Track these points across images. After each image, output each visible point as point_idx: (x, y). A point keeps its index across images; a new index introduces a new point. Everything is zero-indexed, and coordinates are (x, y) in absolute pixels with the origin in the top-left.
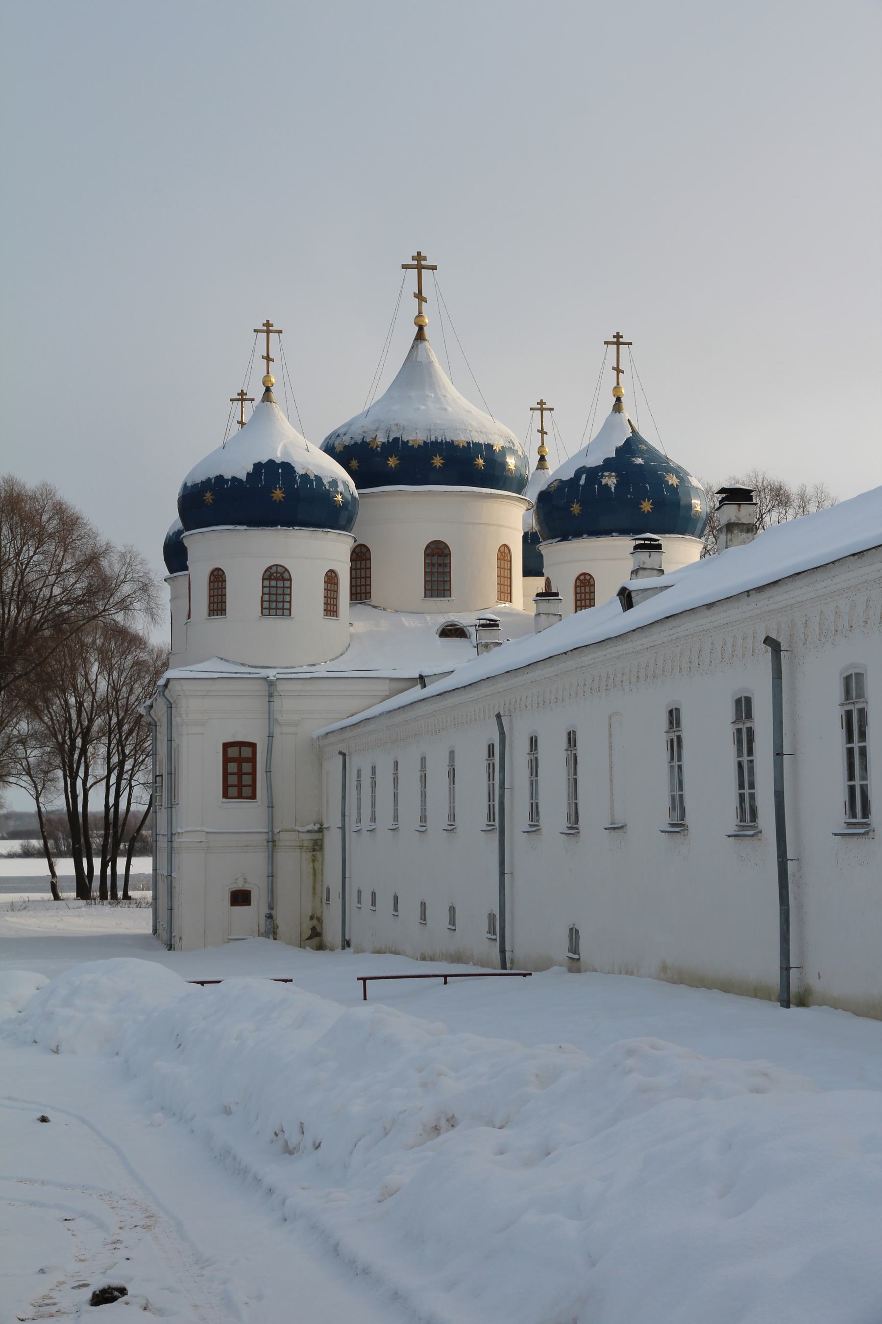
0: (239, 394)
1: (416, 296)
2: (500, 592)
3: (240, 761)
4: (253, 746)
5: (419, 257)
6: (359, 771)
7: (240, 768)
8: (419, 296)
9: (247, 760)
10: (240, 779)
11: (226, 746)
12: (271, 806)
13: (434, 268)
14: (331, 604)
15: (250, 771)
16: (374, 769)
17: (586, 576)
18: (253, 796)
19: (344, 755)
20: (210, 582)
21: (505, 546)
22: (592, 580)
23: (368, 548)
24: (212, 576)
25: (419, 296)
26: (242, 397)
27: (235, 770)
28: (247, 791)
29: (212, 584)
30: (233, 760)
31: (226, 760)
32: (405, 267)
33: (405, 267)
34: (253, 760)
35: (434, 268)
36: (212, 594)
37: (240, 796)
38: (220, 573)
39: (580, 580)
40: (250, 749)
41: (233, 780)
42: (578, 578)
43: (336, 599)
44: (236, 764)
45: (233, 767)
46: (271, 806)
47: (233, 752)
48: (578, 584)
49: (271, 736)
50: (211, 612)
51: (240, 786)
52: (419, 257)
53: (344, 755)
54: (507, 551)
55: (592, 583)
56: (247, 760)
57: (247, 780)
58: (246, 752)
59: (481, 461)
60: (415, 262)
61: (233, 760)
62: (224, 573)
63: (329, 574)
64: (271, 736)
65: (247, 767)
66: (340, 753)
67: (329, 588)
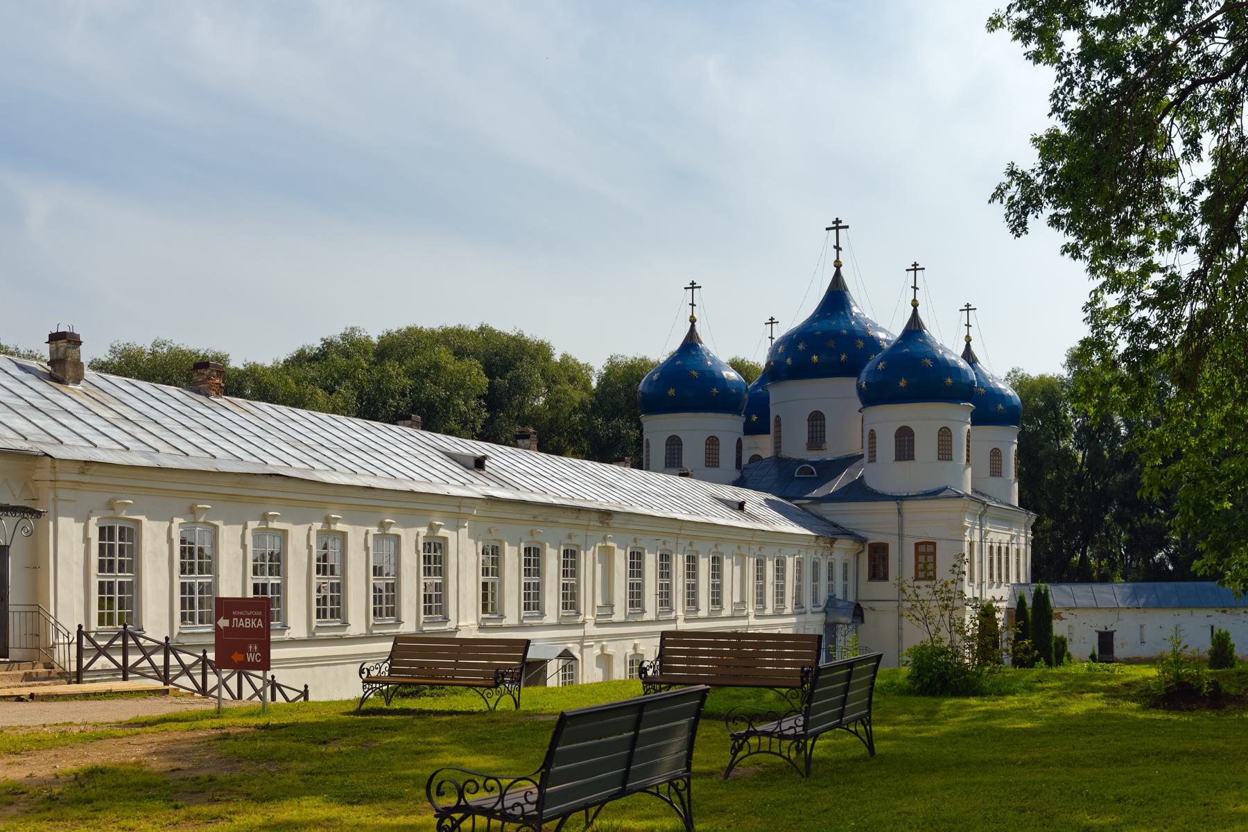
1: (835, 247)
3: (926, 554)
7: (926, 559)
8: (838, 248)
10: (925, 567)
25: (838, 248)
32: (827, 229)
33: (827, 229)
45: (922, 558)
47: (922, 549)
51: (925, 569)
57: (930, 567)
58: (930, 549)
60: (835, 225)
61: (923, 554)
65: (930, 558)
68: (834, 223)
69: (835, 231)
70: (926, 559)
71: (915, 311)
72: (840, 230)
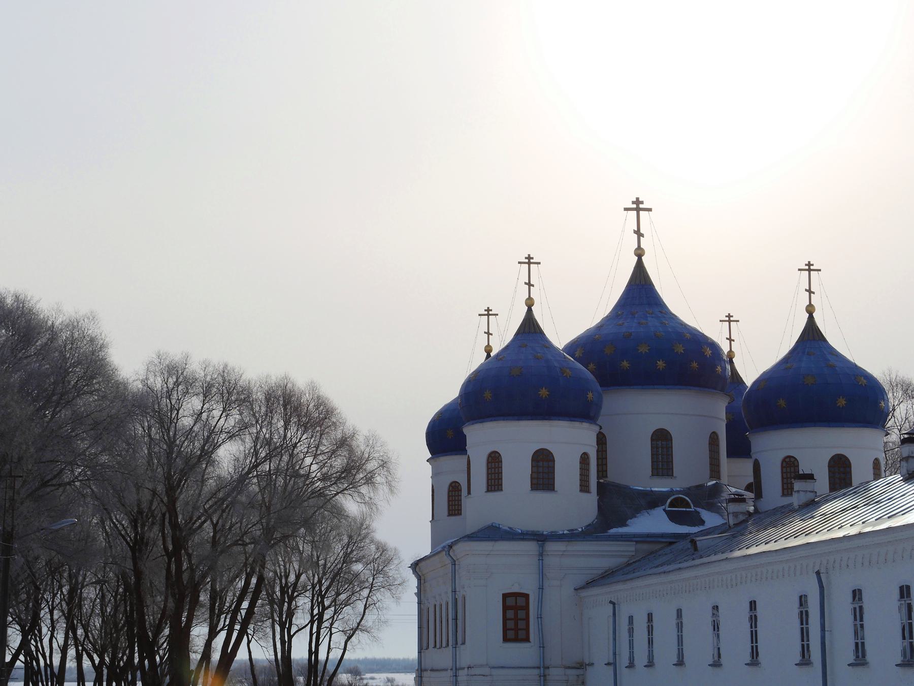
0: (485, 310)
1: (635, 232)
2: (711, 471)
3: (516, 608)
4: (526, 596)
5: (638, 202)
6: (631, 619)
7: (516, 614)
8: (639, 233)
9: (522, 608)
10: (516, 624)
11: (505, 596)
12: (542, 647)
13: (649, 210)
14: (585, 481)
15: (524, 617)
16: (650, 617)
17: (791, 459)
18: (527, 639)
19: (614, 604)
20: (488, 462)
21: (714, 433)
22: (796, 462)
23: (604, 434)
24: (490, 458)
25: (639, 233)
26: (488, 312)
27: (513, 617)
28: (522, 634)
29: (490, 465)
30: (510, 608)
31: (505, 608)
32: (626, 209)
33: (626, 209)
34: (526, 608)
35: (649, 210)
36: (490, 472)
37: (516, 640)
38: (497, 455)
39: (785, 461)
40: (524, 599)
41: (511, 624)
42: (784, 460)
43: (588, 476)
44: (513, 611)
45: (510, 614)
46: (542, 647)
47: (511, 601)
48: (784, 464)
49: (541, 588)
50: (490, 487)
51: (516, 629)
52: (638, 202)
53: (614, 604)
54: (715, 437)
55: (796, 464)
56: (522, 608)
57: (521, 624)
58: (521, 602)
59: (695, 365)
60: (635, 206)
61: (510, 608)
62: (500, 455)
63: (583, 456)
64: (541, 588)
65: (521, 614)
66: (611, 602)
67: (583, 467)
68: (633, 203)
69: (641, 212)
70: (516, 614)
71: (530, 310)
72: (635, 212)
